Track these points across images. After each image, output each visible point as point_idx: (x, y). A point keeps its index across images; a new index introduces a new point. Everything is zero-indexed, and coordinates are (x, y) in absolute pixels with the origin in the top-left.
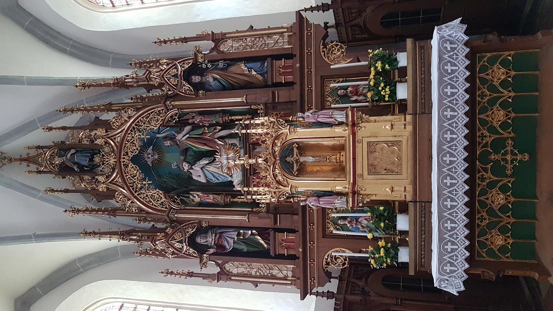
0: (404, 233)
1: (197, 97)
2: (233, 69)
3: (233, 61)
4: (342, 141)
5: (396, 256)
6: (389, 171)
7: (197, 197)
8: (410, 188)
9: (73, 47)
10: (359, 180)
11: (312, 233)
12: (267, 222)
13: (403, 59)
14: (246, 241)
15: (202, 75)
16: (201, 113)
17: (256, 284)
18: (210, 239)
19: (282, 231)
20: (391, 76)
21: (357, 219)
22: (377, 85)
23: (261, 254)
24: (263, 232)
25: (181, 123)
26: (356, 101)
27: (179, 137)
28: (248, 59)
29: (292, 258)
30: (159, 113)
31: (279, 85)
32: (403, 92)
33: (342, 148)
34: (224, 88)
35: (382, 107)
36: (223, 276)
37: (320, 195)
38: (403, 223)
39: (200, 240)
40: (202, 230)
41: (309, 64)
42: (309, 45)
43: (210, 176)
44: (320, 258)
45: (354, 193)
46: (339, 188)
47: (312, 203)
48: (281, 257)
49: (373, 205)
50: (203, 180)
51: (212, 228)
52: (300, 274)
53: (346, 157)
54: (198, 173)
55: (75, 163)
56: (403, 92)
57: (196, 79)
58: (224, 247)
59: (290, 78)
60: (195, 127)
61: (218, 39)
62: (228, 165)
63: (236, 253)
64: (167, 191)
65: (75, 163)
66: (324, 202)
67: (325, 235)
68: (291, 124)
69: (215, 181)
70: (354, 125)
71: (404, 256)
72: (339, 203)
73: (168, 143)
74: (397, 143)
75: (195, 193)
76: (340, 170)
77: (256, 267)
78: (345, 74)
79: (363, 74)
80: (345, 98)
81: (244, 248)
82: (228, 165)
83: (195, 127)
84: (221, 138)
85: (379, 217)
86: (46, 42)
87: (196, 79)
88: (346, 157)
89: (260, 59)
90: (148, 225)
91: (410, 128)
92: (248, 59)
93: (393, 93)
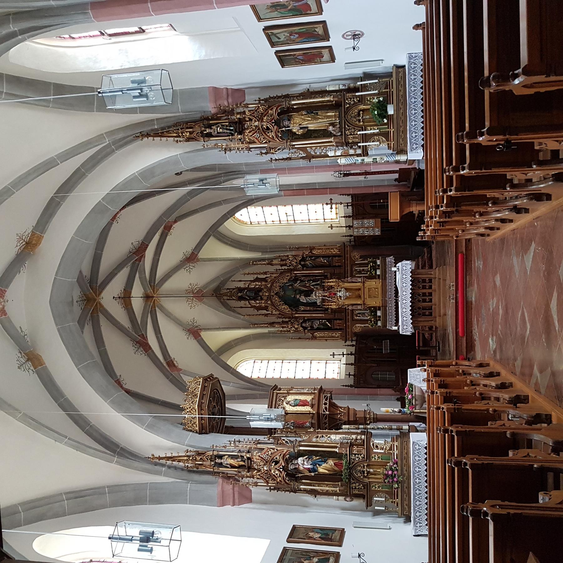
0: (379, 317)
1: (303, 270)
2: (318, 260)
3: (318, 257)
5: (377, 324)
6: (375, 297)
7: (302, 308)
8: (381, 302)
9: (231, 241)
10: (365, 301)
11: (348, 319)
12: (331, 316)
13: (378, 262)
14: (322, 324)
15: (304, 261)
16: (303, 276)
17: (326, 340)
18: (308, 324)
19: (336, 320)
20: (375, 268)
21: (364, 313)
22: (371, 270)
23: (327, 329)
24: (329, 320)
25: (296, 280)
26: (364, 274)
27: (296, 285)
28: (323, 257)
29: (340, 329)
30: (288, 276)
31: (335, 266)
32: (378, 272)
33: (360, 289)
34: (313, 267)
35: (373, 277)
36: (314, 338)
37: (353, 305)
38: (379, 313)
39: (304, 325)
40: (305, 321)
41: (347, 260)
42: (347, 254)
43: (308, 300)
44: (352, 328)
45: (364, 304)
46: (359, 303)
47: (350, 308)
48: (337, 329)
49: (370, 308)
50: (305, 301)
51: (309, 320)
52: (344, 335)
53: (361, 293)
54: (303, 299)
55: (247, 295)
56: (378, 272)
57: (302, 263)
58: (313, 327)
59: (340, 264)
60: (302, 281)
61: (312, 249)
62: (317, 297)
63: (318, 329)
64: (290, 306)
65: (247, 295)
66: (354, 307)
67: (353, 320)
68: (343, 282)
69: (310, 302)
70: (364, 282)
71: (379, 324)
72: (359, 307)
73: (290, 287)
74: (377, 288)
75: (301, 307)
76: (359, 297)
77: (326, 333)
78: (360, 265)
79: (366, 265)
80: (360, 272)
81: (322, 327)
82: (317, 297)
83: (302, 281)
84: (312, 286)
85: (372, 312)
86: (219, 240)
87: (302, 263)
88: (361, 293)
89: (329, 257)
90: (280, 320)
91: (381, 284)
92: (323, 257)
93: (376, 273)
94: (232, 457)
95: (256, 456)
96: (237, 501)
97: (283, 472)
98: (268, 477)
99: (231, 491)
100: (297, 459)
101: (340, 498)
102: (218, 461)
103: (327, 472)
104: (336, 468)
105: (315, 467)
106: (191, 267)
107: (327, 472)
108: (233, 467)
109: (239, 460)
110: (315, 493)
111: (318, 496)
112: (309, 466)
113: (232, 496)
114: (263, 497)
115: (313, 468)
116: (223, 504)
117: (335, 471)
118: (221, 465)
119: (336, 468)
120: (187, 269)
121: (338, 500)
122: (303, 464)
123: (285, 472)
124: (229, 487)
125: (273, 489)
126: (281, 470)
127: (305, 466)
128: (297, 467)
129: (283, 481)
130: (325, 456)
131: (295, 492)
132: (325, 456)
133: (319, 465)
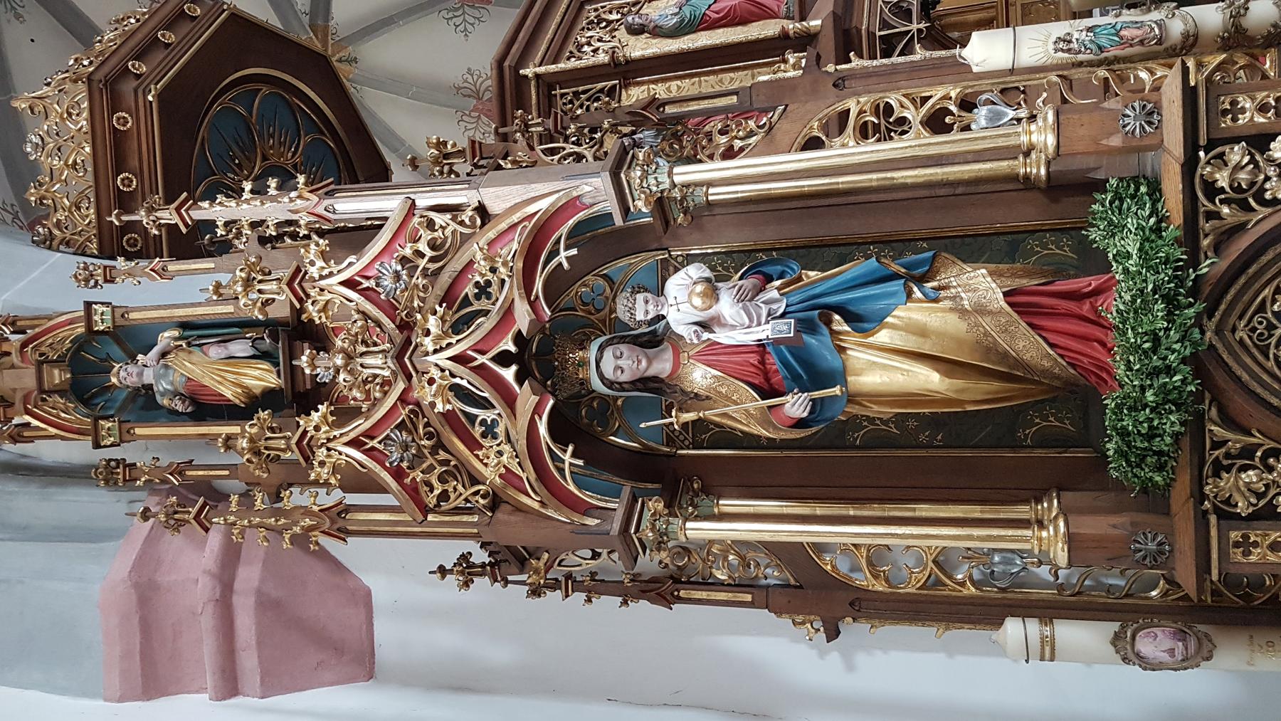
4: (992, 13)
94: (195, 331)
95: (332, 287)
96: (249, 661)
97: (526, 397)
98: (426, 467)
99: (202, 591)
100: (660, 291)
101: (1069, 632)
102: (124, 375)
103: (929, 379)
104: (1028, 345)
105: (818, 344)
106: (472, 21)
107: (929, 379)
108: (205, 408)
109: (240, 348)
110: (815, 595)
111: (852, 630)
112: (765, 332)
113: (207, 622)
114: (443, 641)
115: (794, 347)
116: (152, 676)
117: (1009, 370)
118: (144, 403)
119: (1028, 345)
120: (458, 20)
121: (1049, 650)
122: (705, 318)
123: (542, 388)
124: (192, 560)
125: (482, 569)
126: (509, 374)
127: (723, 337)
128: (662, 366)
129: (528, 474)
130: (909, 234)
131: (664, 589)
132: (909, 234)
133: (852, 318)
